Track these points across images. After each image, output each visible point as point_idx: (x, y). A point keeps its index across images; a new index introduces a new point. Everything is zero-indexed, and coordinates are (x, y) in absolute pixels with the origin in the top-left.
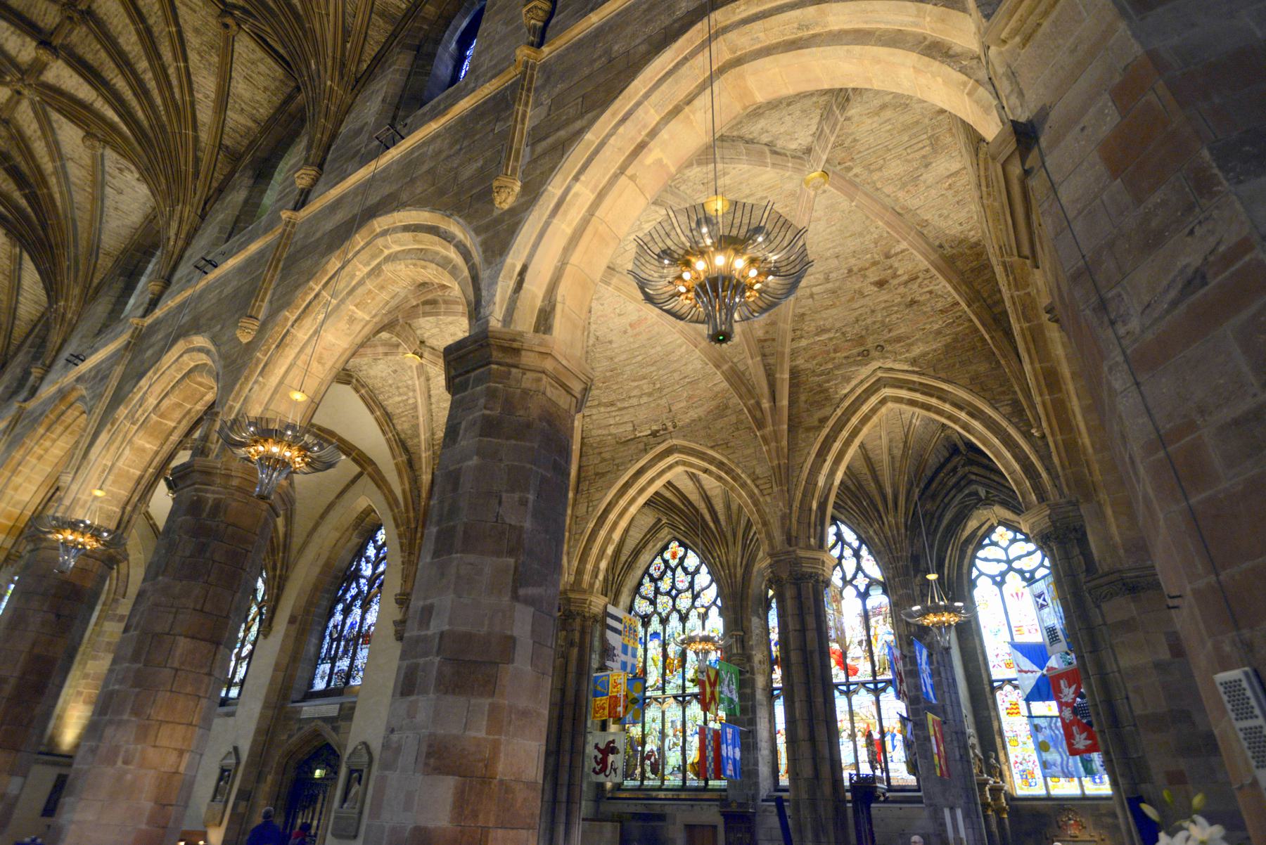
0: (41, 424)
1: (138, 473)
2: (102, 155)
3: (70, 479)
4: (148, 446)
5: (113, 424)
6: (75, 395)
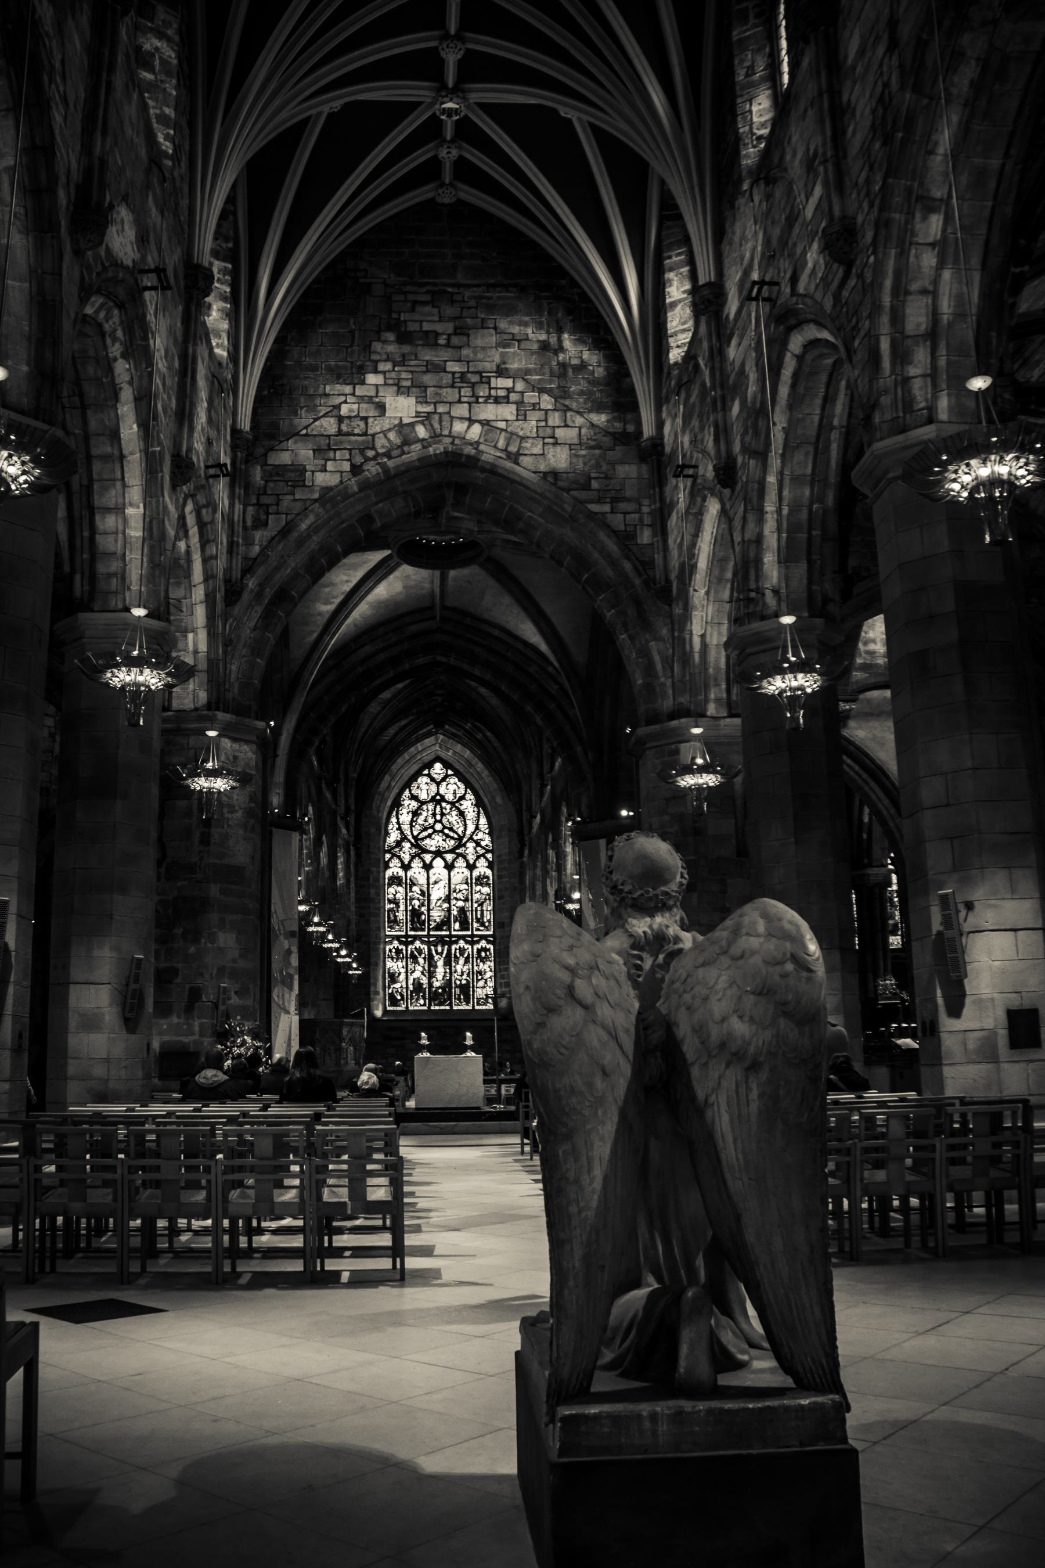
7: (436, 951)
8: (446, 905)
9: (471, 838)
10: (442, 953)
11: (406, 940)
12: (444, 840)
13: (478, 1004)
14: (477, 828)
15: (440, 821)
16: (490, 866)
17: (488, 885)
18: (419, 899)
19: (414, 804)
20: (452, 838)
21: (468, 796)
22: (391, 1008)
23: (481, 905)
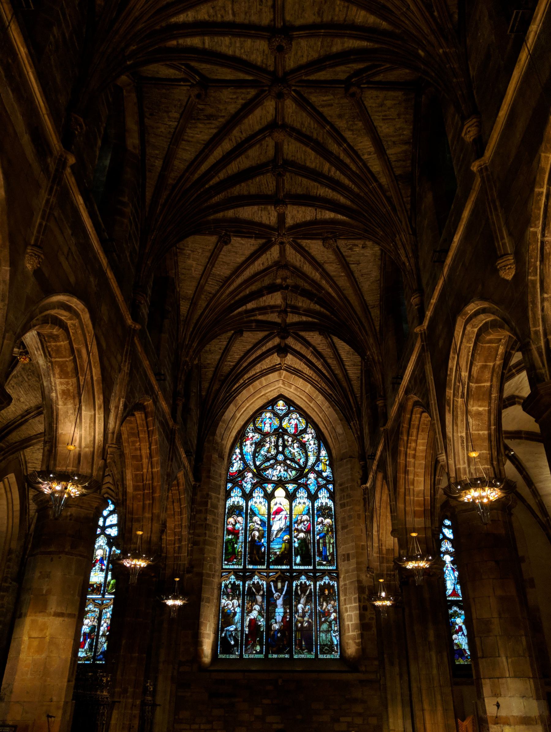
0: (402, 433)
1: (486, 432)
2: (337, 247)
3: (445, 457)
4: (481, 409)
5: (449, 406)
6: (410, 404)
7: (276, 587)
8: (287, 537)
9: (312, 470)
10: (281, 591)
11: (244, 575)
12: (286, 471)
13: (322, 653)
14: (318, 460)
15: (283, 453)
16: (332, 497)
17: (329, 516)
18: (258, 530)
19: (257, 436)
20: (294, 469)
21: (309, 430)
22: (223, 656)
23: (324, 537)
